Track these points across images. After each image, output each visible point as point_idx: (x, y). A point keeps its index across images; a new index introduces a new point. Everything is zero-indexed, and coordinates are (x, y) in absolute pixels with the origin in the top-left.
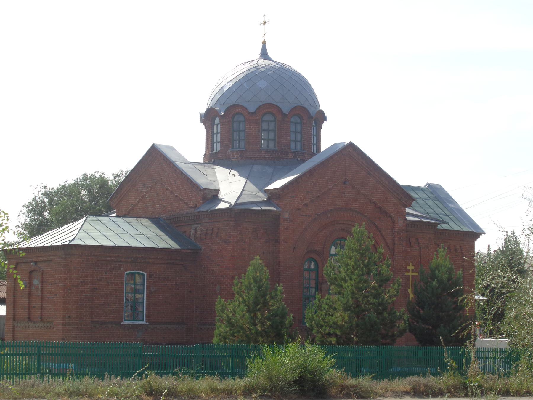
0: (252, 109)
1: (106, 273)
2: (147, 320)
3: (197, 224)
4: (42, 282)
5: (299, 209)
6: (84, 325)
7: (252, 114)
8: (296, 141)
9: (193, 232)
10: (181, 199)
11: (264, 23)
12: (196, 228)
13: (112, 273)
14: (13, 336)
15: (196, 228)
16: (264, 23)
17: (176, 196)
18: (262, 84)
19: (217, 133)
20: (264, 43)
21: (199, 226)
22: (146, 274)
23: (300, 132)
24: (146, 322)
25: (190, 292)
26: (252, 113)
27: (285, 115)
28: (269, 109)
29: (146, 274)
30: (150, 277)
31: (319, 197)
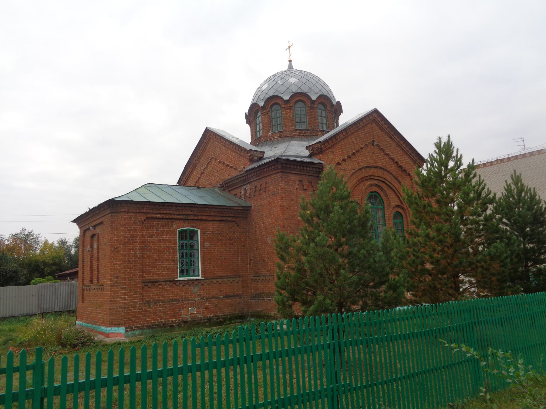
0: (286, 98)
1: (157, 230)
2: (203, 275)
3: (246, 184)
4: (98, 245)
5: (338, 164)
6: (133, 285)
7: (287, 101)
8: (323, 124)
9: (243, 192)
10: (231, 167)
11: (289, 47)
12: (245, 189)
13: (164, 231)
14: (83, 298)
15: (245, 189)
16: (289, 47)
17: (227, 165)
18: (293, 80)
19: (259, 131)
20: (290, 61)
21: (248, 185)
22: (199, 231)
23: (325, 117)
24: (202, 277)
25: (244, 246)
26: (286, 100)
27: (313, 102)
28: (300, 97)
29: (199, 231)
30: (203, 233)
31: (354, 154)
